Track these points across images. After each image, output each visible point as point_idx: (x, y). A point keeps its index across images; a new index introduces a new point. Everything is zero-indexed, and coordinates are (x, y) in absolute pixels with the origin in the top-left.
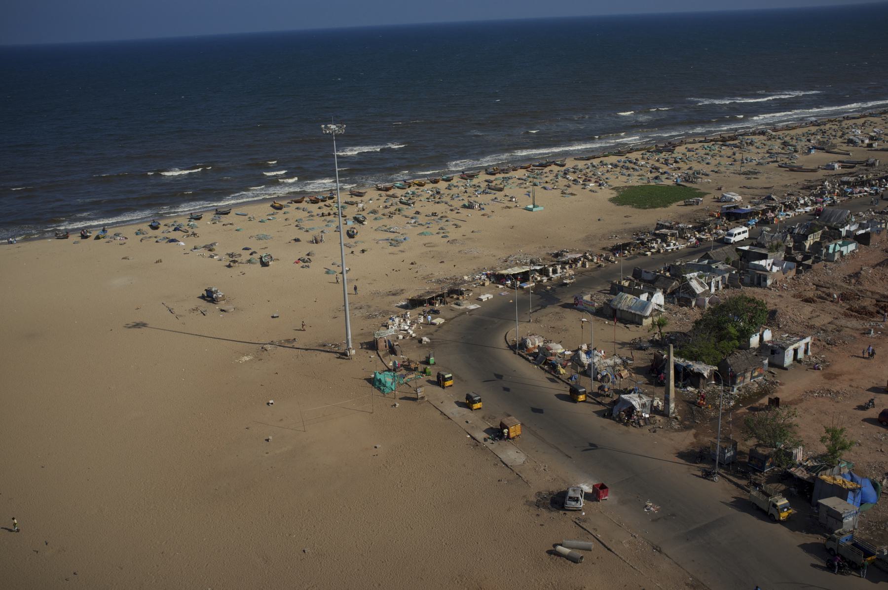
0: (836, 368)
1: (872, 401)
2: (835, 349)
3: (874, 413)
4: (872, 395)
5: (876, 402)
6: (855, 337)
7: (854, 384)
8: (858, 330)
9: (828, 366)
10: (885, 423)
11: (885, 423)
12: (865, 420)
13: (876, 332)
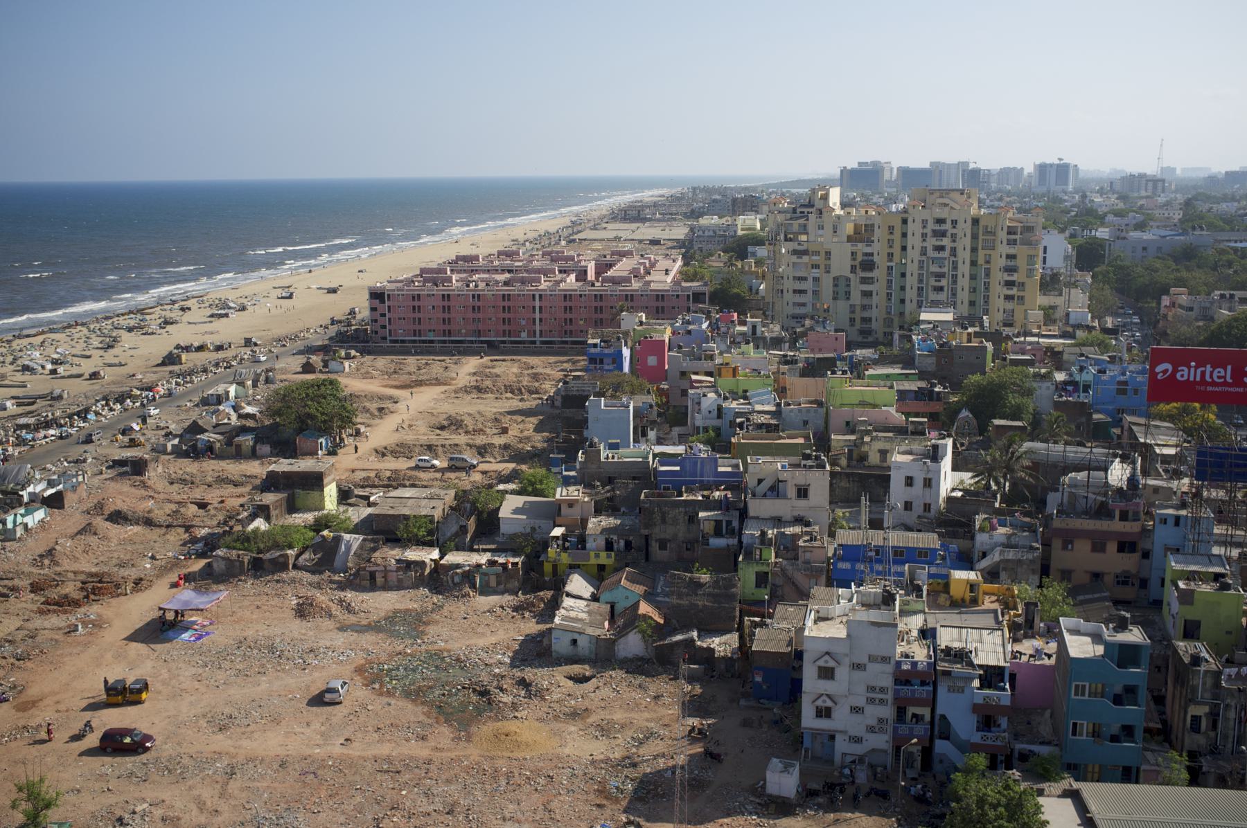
0: (33, 692)
1: (88, 724)
2: (29, 664)
3: (93, 740)
4: (88, 715)
5: (93, 724)
6: (56, 641)
7: (62, 707)
8: (60, 629)
9: (21, 692)
10: (109, 750)
11: (109, 750)
12: (81, 754)
13: (85, 624)
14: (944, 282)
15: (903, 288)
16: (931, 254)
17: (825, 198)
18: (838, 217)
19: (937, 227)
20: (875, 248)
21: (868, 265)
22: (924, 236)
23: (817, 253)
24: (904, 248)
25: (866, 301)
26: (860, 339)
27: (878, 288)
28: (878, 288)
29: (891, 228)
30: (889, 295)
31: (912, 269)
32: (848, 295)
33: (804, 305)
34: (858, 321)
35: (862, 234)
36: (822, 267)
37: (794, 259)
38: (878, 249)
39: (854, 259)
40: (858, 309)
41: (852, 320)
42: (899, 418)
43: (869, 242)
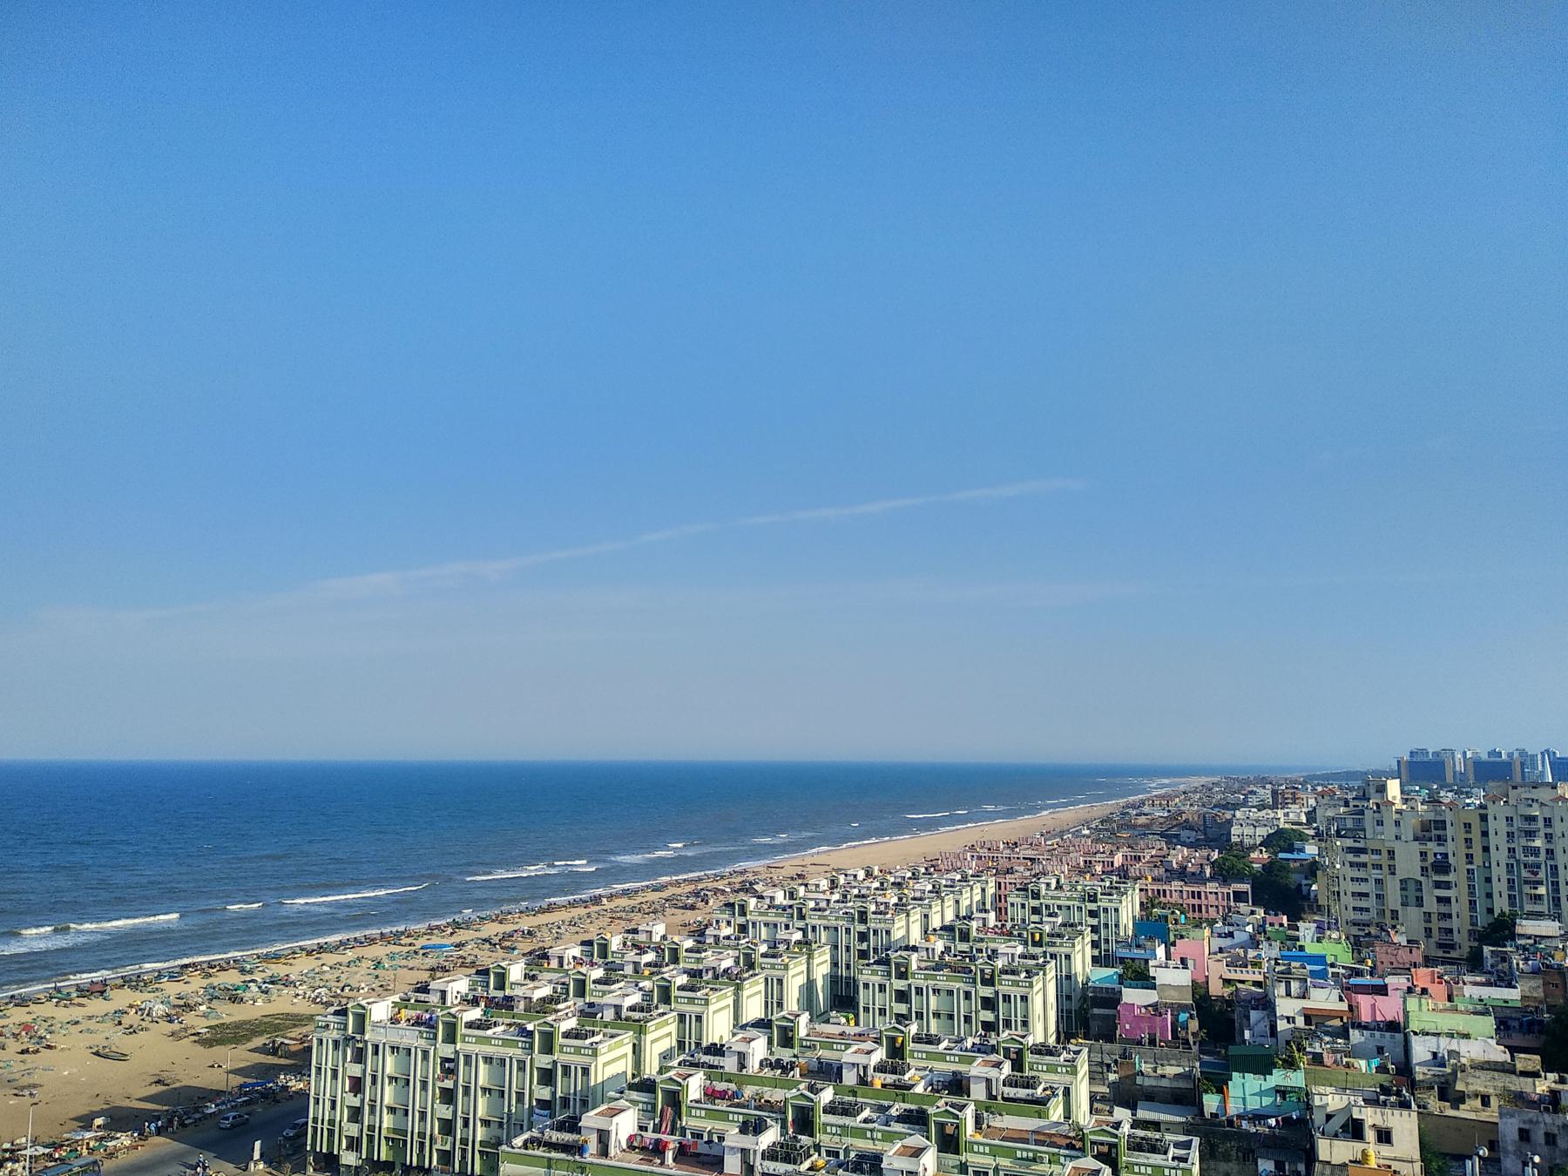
14: (1542, 890)
15: (1489, 896)
16: (1520, 855)
17: (1382, 789)
18: (1399, 812)
19: (1526, 826)
20: (1450, 847)
21: (1442, 866)
22: (1510, 835)
23: (1378, 852)
24: (1486, 849)
25: (1444, 909)
26: (1440, 953)
27: (1458, 894)
28: (1458, 894)
29: (1468, 826)
30: (1472, 903)
31: (1499, 872)
32: (1420, 902)
33: (1367, 910)
34: (1435, 932)
35: (1432, 830)
36: (1385, 868)
37: (1351, 857)
38: (1454, 848)
39: (1424, 860)
40: (1434, 918)
41: (1428, 931)
42: (1499, 1054)
43: (1441, 840)
